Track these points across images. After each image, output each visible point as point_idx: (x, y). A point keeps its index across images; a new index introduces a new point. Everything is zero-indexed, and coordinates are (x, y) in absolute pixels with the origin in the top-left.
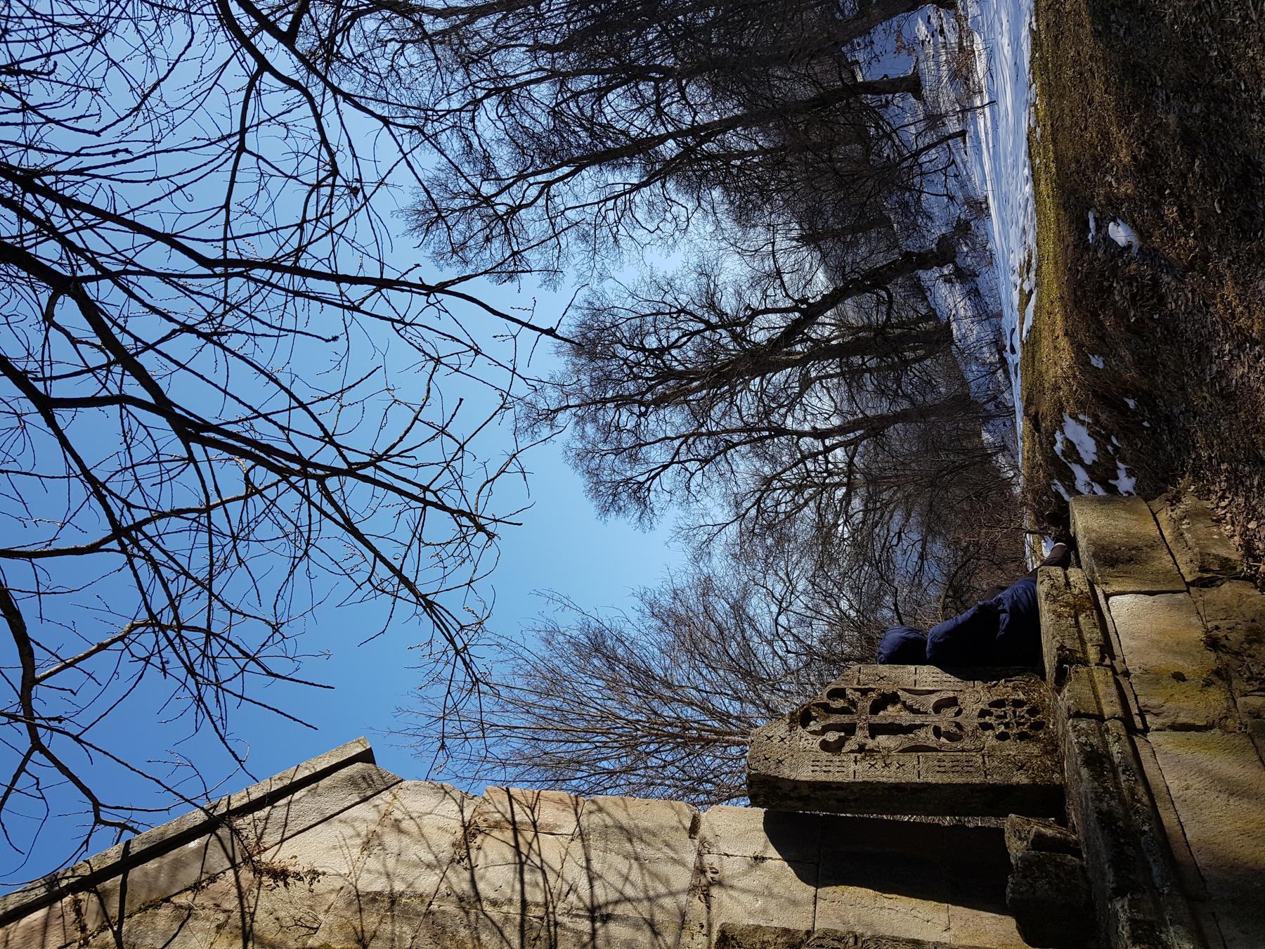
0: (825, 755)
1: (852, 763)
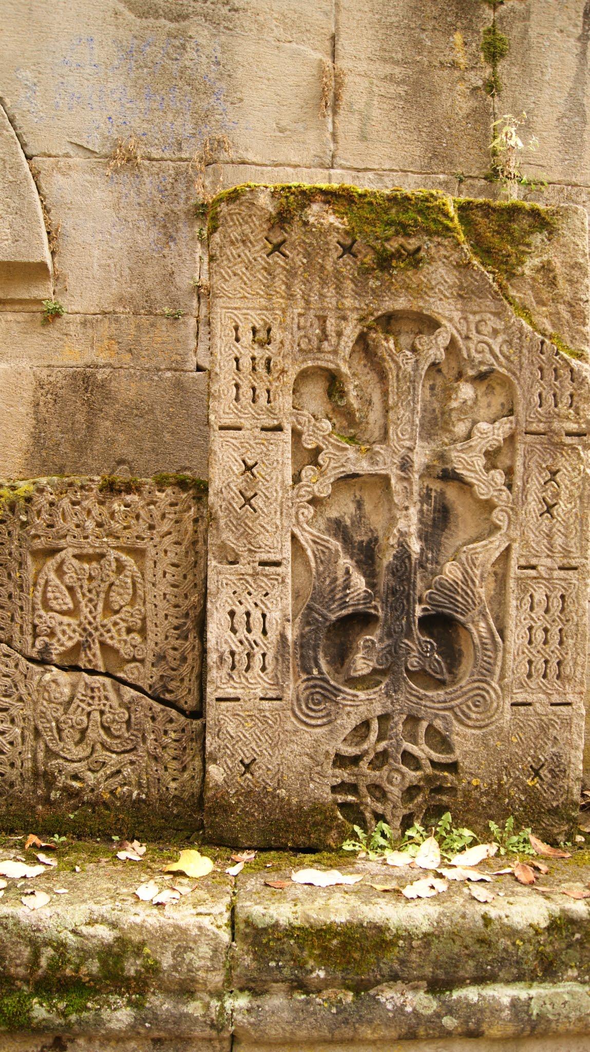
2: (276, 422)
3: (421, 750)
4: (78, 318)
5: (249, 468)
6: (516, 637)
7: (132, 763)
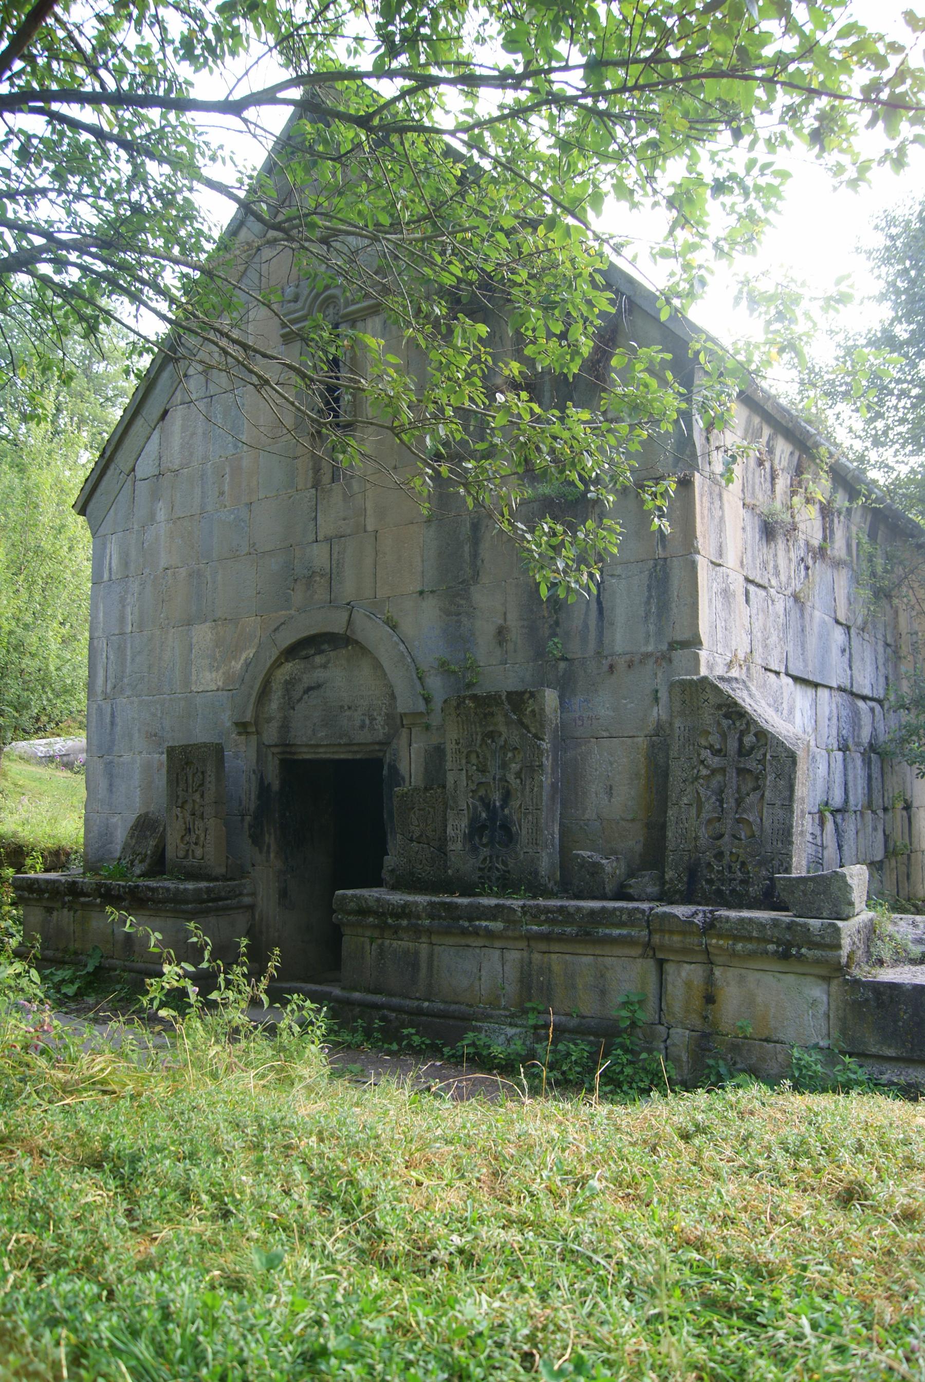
3: (500, 866)
6: (524, 832)
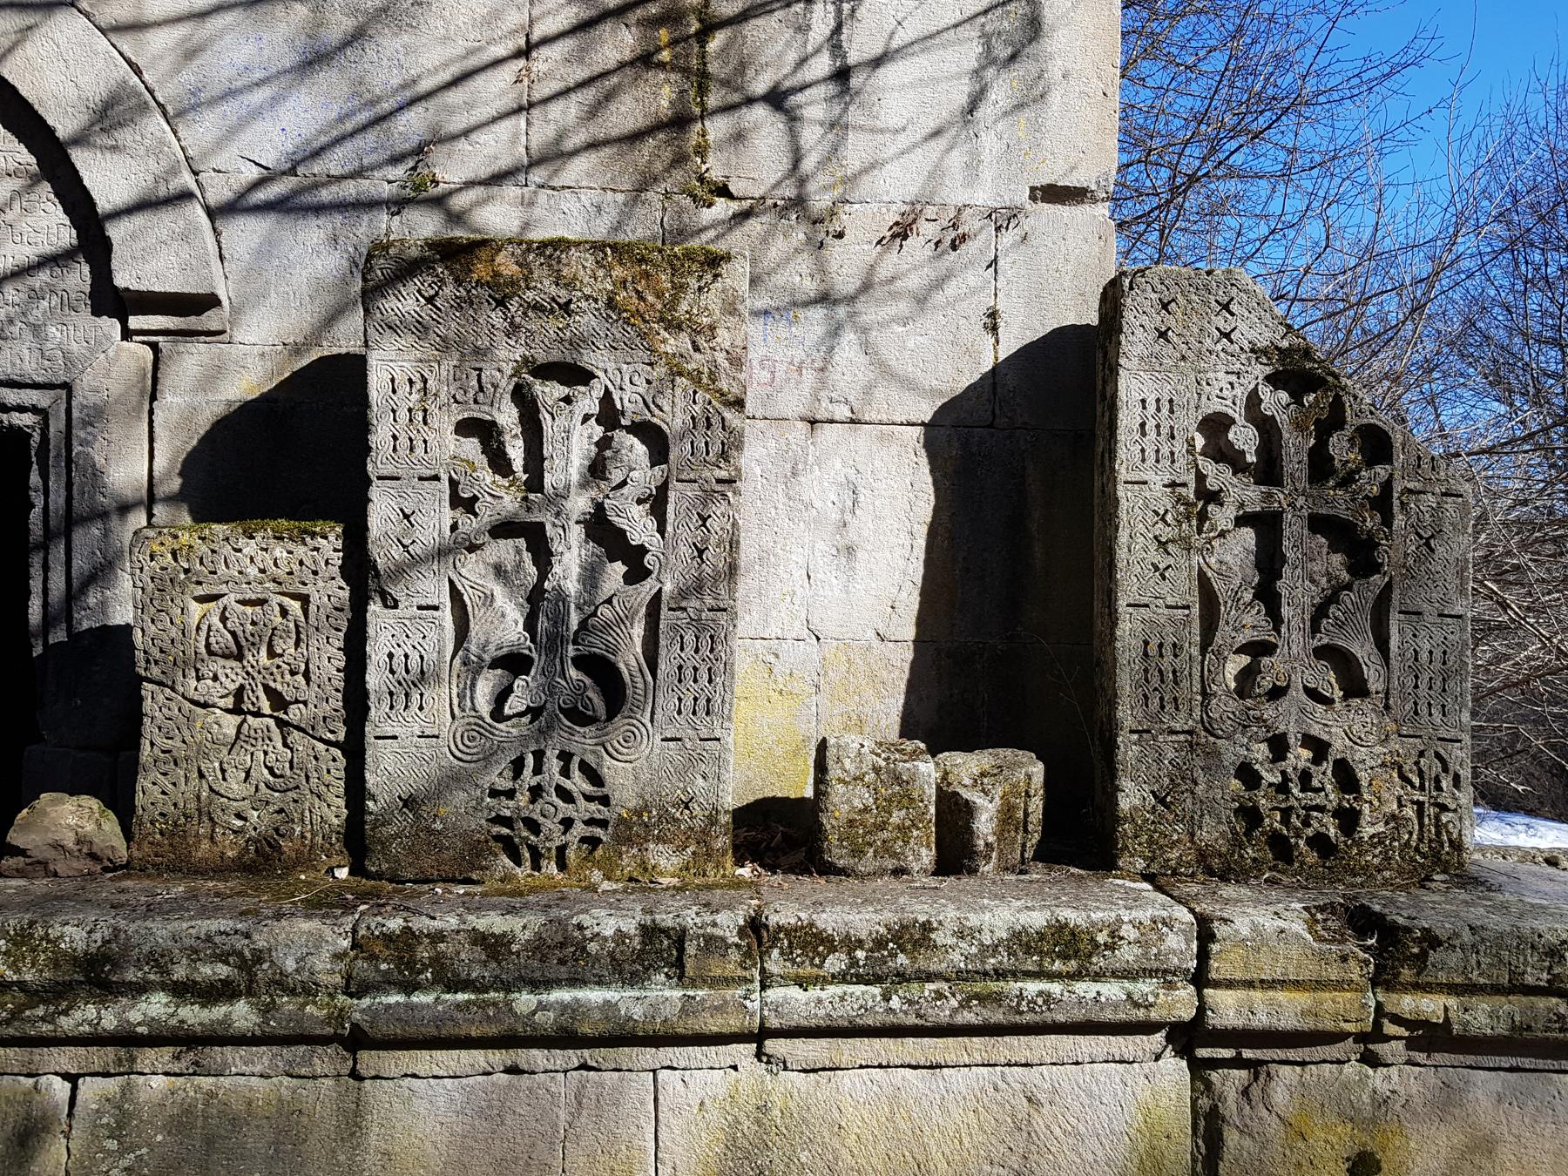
0: (1188, 422)
1: (1167, 479)
2: (433, 473)
4: (256, 349)
5: (406, 517)
7: (295, 801)
